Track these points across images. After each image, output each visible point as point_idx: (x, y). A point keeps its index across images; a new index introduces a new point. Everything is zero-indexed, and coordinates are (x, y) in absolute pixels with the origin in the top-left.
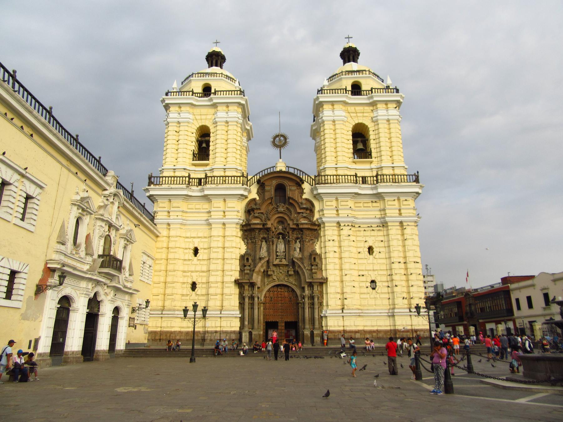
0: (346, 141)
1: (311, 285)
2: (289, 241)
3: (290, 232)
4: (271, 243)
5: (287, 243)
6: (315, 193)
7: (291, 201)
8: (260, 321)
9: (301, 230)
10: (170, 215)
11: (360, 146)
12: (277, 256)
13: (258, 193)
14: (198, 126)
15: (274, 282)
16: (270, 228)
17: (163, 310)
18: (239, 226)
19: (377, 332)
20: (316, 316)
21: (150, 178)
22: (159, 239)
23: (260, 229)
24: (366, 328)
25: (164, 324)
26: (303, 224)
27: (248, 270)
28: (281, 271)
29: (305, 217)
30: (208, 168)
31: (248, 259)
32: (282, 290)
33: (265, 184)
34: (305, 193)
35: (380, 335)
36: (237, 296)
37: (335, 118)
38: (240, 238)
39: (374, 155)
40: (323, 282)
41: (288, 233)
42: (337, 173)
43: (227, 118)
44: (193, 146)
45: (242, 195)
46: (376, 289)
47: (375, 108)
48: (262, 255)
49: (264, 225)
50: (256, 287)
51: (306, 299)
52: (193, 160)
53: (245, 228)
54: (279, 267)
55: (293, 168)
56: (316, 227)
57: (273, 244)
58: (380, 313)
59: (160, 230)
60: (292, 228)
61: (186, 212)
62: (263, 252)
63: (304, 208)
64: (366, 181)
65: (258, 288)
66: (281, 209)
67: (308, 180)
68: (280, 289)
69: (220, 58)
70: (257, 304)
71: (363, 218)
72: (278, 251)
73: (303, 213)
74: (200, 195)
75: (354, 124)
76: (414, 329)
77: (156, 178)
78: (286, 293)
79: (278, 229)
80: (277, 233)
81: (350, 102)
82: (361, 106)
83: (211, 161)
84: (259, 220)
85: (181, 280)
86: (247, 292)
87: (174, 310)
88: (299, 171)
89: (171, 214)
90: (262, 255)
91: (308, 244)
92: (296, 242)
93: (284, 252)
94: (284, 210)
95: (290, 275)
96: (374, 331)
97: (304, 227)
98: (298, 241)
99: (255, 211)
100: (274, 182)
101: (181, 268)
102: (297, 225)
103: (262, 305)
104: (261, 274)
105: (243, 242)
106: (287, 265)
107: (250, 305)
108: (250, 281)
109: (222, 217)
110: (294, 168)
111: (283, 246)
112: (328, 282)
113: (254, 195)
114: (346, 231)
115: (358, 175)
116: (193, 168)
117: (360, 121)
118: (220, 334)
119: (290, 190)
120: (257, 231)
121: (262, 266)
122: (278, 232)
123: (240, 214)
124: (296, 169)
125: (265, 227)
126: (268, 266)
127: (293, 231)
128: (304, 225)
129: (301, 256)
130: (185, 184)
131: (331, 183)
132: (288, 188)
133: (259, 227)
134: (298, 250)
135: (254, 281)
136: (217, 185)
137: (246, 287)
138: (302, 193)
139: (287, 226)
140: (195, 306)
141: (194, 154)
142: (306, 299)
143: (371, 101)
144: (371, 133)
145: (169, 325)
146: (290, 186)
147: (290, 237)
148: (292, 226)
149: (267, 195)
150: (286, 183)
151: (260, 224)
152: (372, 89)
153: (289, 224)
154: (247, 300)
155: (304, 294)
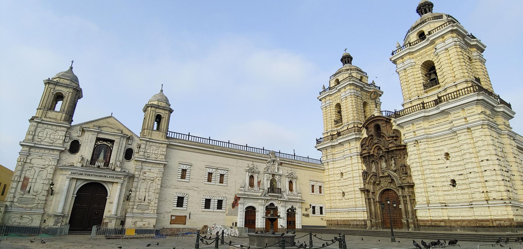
0: (417, 79)
1: (402, 188)
3: (386, 154)
4: (376, 163)
5: (386, 161)
6: (396, 125)
7: (382, 134)
9: (392, 151)
11: (433, 77)
12: (383, 171)
13: (367, 134)
14: (335, 105)
15: (382, 188)
16: (373, 154)
18: (359, 157)
19: (461, 221)
20: (409, 209)
22: (325, 171)
23: (369, 156)
24: (451, 218)
26: (391, 147)
29: (391, 143)
30: (341, 127)
32: (391, 193)
33: (368, 127)
34: (393, 126)
35: (464, 224)
36: (364, 198)
40: (412, 186)
43: (345, 95)
44: (334, 117)
45: (355, 138)
46: (457, 186)
49: (369, 153)
50: (370, 192)
53: (362, 157)
54: (384, 178)
56: (403, 147)
57: (378, 164)
58: (463, 205)
59: (325, 167)
60: (385, 152)
61: (335, 154)
62: (374, 170)
65: (373, 193)
66: (376, 141)
69: (347, 58)
70: (373, 203)
71: (436, 133)
73: (390, 140)
76: (494, 219)
78: (394, 194)
81: (414, 50)
82: (424, 49)
83: (343, 122)
84: (366, 150)
85: (338, 191)
87: (336, 208)
88: (388, 112)
89: (328, 157)
91: (400, 160)
93: (386, 167)
94: (377, 142)
95: (391, 183)
96: (459, 221)
97: (392, 149)
98: (392, 159)
99: (364, 146)
100: (373, 124)
101: (337, 185)
102: (388, 149)
104: (372, 184)
106: (388, 176)
109: (349, 153)
110: (385, 111)
112: (415, 185)
113: (365, 135)
115: (425, 102)
116: (336, 129)
117: (425, 60)
119: (383, 127)
120: (368, 158)
122: (380, 155)
123: (359, 149)
125: (371, 154)
126: (376, 179)
128: (392, 148)
129: (395, 169)
131: (404, 115)
132: (381, 126)
134: (393, 165)
135: (367, 189)
138: (392, 126)
141: (335, 121)
142: (401, 198)
147: (386, 157)
148: (385, 150)
149: (370, 134)
150: (380, 123)
151: (367, 153)
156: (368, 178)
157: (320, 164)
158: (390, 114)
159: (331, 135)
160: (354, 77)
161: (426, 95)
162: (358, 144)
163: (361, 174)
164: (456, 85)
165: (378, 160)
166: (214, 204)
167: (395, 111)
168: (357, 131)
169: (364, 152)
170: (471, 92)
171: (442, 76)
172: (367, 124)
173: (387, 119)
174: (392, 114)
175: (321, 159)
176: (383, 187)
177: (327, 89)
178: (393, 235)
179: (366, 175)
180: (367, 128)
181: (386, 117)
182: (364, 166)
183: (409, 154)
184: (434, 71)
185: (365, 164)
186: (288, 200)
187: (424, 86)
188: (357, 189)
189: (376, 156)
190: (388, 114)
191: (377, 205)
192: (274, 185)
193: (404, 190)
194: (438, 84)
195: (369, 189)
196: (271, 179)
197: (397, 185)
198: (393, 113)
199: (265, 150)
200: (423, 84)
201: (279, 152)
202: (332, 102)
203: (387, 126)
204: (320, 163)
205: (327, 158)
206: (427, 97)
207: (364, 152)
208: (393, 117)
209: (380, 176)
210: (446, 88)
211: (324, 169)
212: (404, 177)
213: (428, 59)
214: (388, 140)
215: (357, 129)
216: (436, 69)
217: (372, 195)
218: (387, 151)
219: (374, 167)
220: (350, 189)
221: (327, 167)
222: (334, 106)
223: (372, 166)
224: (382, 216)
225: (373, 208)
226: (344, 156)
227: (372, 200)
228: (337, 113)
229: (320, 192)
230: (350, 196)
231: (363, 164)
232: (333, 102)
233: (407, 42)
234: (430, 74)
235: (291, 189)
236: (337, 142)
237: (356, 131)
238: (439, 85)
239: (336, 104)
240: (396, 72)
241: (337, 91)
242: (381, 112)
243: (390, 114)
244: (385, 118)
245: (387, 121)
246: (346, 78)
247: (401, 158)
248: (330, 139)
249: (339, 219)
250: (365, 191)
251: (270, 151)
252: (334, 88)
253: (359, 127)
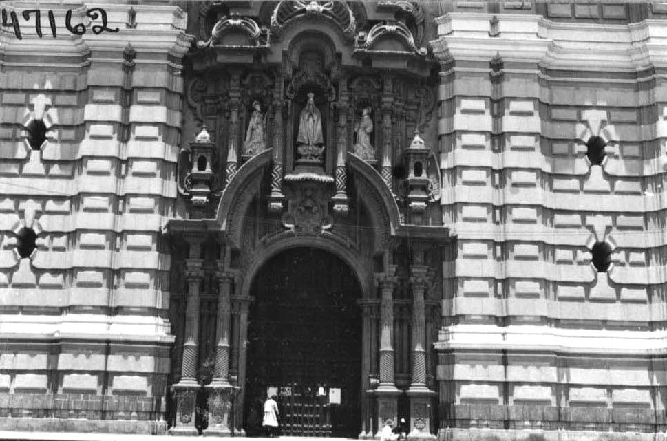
2: (337, 112)
5: (330, 118)
9: (379, 75)
12: (299, 156)
16: (276, 66)
23: (245, 70)
41: (336, 85)
48: (248, 151)
50: (228, 248)
51: (388, 295)
65: (235, 254)
72: (299, 140)
79: (305, 75)
80: (299, 85)
90: (248, 151)
92: (359, 116)
93: (320, 145)
98: (365, 112)
107: (205, 304)
111: (319, 127)
125: (263, 60)
127: (350, 81)
137: (194, 251)
139: (333, 64)
142: (388, 295)
148: (347, 60)
153: (339, 56)
154: (194, 290)
155: (382, 279)
176: (293, 230)
189: (287, 82)
217: (232, 266)
219: (259, 130)
223: (253, 123)
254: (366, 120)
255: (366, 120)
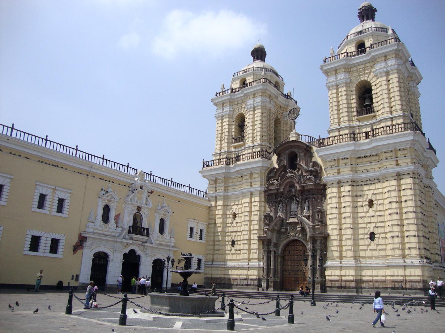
4: (284, 205)
5: (298, 203)
8: (277, 271)
9: (309, 191)
10: (217, 189)
12: (292, 215)
14: (236, 115)
17: (213, 261)
18: (263, 193)
21: (203, 163)
23: (276, 195)
25: (213, 272)
27: (267, 228)
28: (293, 228)
29: (309, 179)
31: (267, 219)
32: (297, 244)
37: (337, 82)
38: (265, 202)
39: (376, 109)
40: (326, 238)
42: (339, 133)
43: (253, 104)
47: (376, 63)
49: (278, 190)
50: (273, 242)
52: (233, 144)
53: (267, 194)
55: (305, 135)
56: (322, 187)
57: (286, 206)
63: (306, 172)
64: (369, 136)
66: (289, 175)
67: (317, 144)
68: (296, 243)
72: (291, 211)
74: (235, 171)
75: (357, 83)
77: (211, 162)
78: (300, 247)
80: (290, 196)
86: (265, 247)
91: (316, 202)
93: (297, 211)
94: (292, 175)
96: (371, 281)
97: (309, 188)
98: (307, 201)
100: (287, 151)
102: (303, 187)
103: (279, 257)
105: (267, 205)
106: (298, 222)
108: (266, 238)
110: (306, 136)
114: (346, 188)
118: (248, 280)
121: (276, 225)
122: (291, 195)
124: (307, 135)
125: (279, 191)
126: (282, 225)
127: (302, 193)
129: (308, 214)
130: (224, 164)
132: (298, 154)
133: (274, 192)
135: (269, 238)
136: (244, 161)
140: (168, 258)
143: (370, 57)
144: (373, 88)
145: (216, 273)
146: (299, 153)
148: (298, 188)
150: (296, 151)
152: (371, 45)
156: (273, 224)
157: (205, 197)
158: (312, 141)
159: (226, 158)
160: (268, 80)
161: (357, 123)
162: (264, 177)
163: (263, 217)
164: (392, 118)
165: (288, 200)
166: (45, 245)
167: (320, 138)
168: (265, 157)
169: (271, 187)
170: (408, 130)
171: (379, 103)
172: (280, 149)
173: (307, 146)
174: (314, 140)
175: (206, 190)
177: (229, 90)
178: (313, 299)
179: (269, 219)
180: (279, 155)
181: (306, 143)
182: (267, 206)
183: (328, 197)
184: (370, 94)
185: (269, 204)
186: (156, 246)
187: (357, 112)
188: (256, 237)
189: (286, 195)
190: (308, 140)
191: (278, 260)
192: (138, 222)
193: (315, 242)
194: (373, 112)
195: (271, 238)
196: (135, 212)
197: (308, 236)
198: (316, 140)
199: (130, 168)
200: (356, 109)
201: (150, 173)
202: (233, 110)
203: (306, 156)
204: (205, 196)
205: (216, 190)
206: (359, 126)
207: (271, 187)
208: (314, 146)
209: (288, 222)
210: (381, 120)
211: (210, 206)
212: (318, 225)
213: (366, 79)
214: (305, 174)
215: (265, 154)
216: (373, 93)
218: (302, 189)
220: (242, 238)
221: (213, 205)
222: (235, 117)
223: (279, 207)
224: (282, 275)
225: (272, 263)
226: (241, 191)
227: (272, 253)
228: (237, 128)
229: (201, 239)
230: (242, 247)
231: (266, 204)
232: (234, 111)
233: (344, 51)
234: (365, 99)
235: (162, 231)
236: (234, 170)
237: (264, 157)
238: (373, 114)
239: (238, 113)
240: (326, 86)
241: (242, 95)
242: (299, 135)
243: (312, 141)
244: (306, 144)
245: (307, 150)
246: (259, 80)
247: (317, 201)
248: (225, 163)
249: (223, 276)
250: (264, 242)
251: (137, 170)
252: (239, 91)
253: (267, 152)
254: (307, 203)
255: (307, 203)
